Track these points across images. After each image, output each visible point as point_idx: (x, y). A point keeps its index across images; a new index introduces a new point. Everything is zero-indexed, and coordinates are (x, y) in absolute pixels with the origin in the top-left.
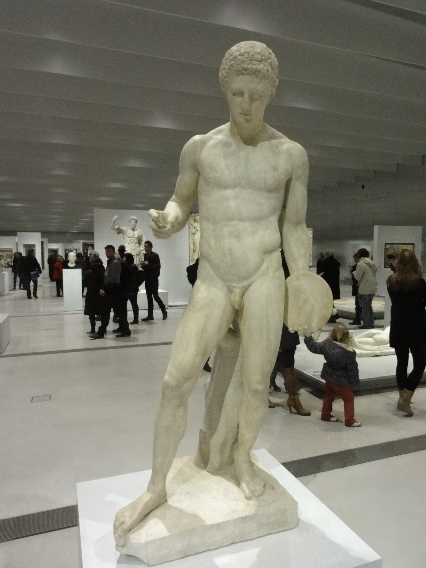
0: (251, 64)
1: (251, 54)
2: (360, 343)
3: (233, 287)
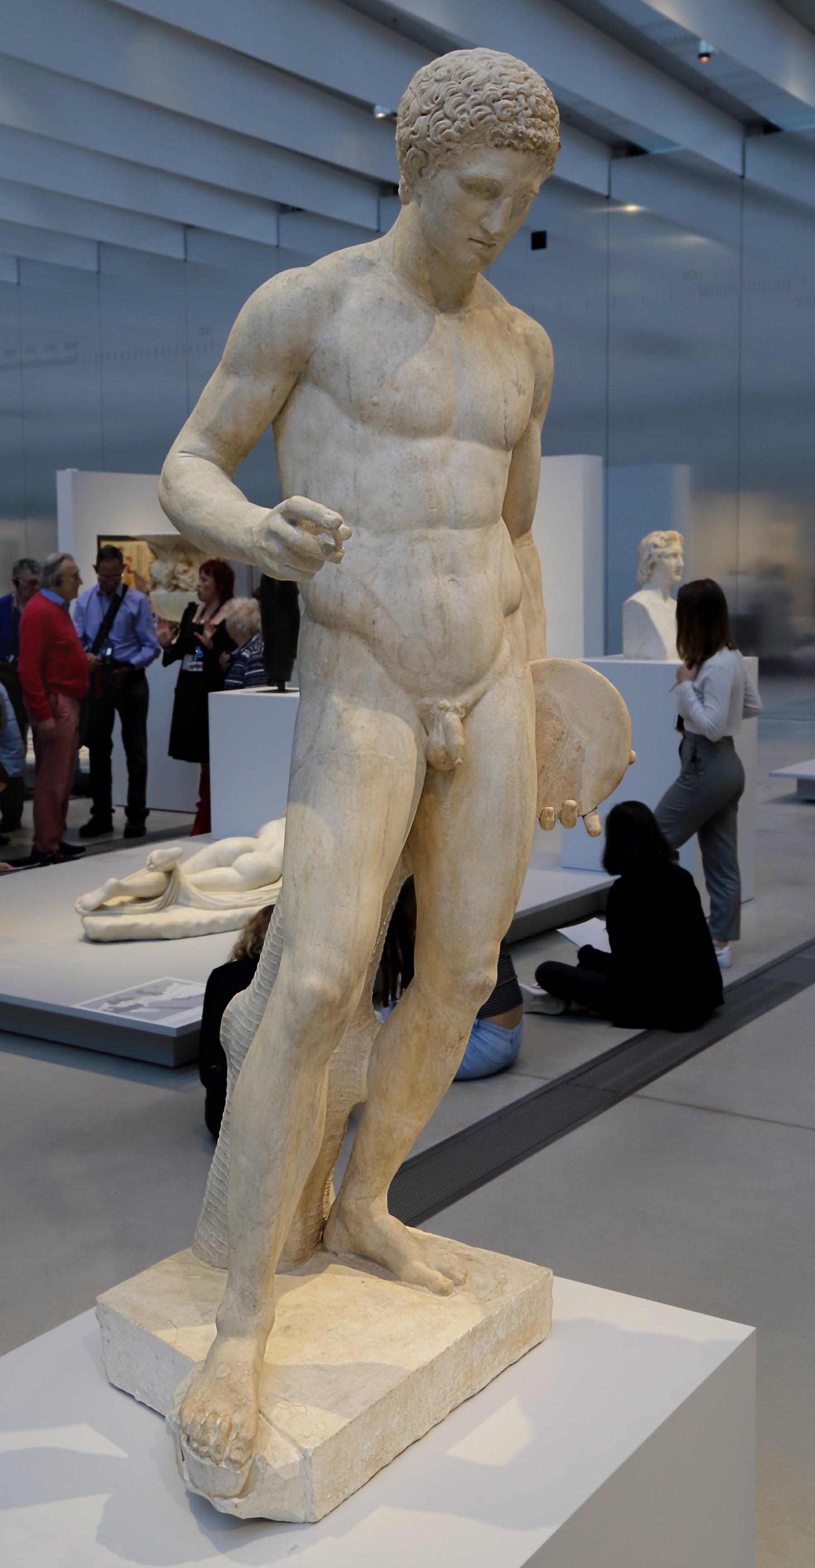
0: (533, 125)
1: (533, 99)
2: (200, 886)
3: (441, 709)
